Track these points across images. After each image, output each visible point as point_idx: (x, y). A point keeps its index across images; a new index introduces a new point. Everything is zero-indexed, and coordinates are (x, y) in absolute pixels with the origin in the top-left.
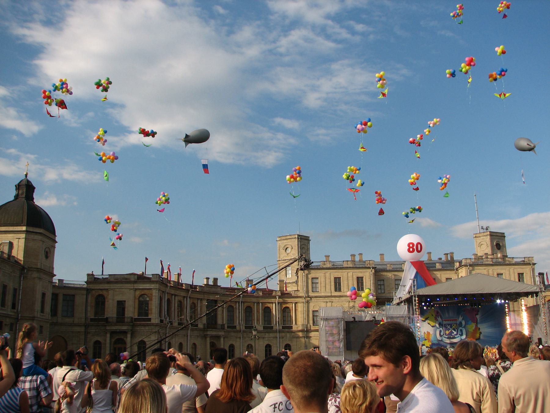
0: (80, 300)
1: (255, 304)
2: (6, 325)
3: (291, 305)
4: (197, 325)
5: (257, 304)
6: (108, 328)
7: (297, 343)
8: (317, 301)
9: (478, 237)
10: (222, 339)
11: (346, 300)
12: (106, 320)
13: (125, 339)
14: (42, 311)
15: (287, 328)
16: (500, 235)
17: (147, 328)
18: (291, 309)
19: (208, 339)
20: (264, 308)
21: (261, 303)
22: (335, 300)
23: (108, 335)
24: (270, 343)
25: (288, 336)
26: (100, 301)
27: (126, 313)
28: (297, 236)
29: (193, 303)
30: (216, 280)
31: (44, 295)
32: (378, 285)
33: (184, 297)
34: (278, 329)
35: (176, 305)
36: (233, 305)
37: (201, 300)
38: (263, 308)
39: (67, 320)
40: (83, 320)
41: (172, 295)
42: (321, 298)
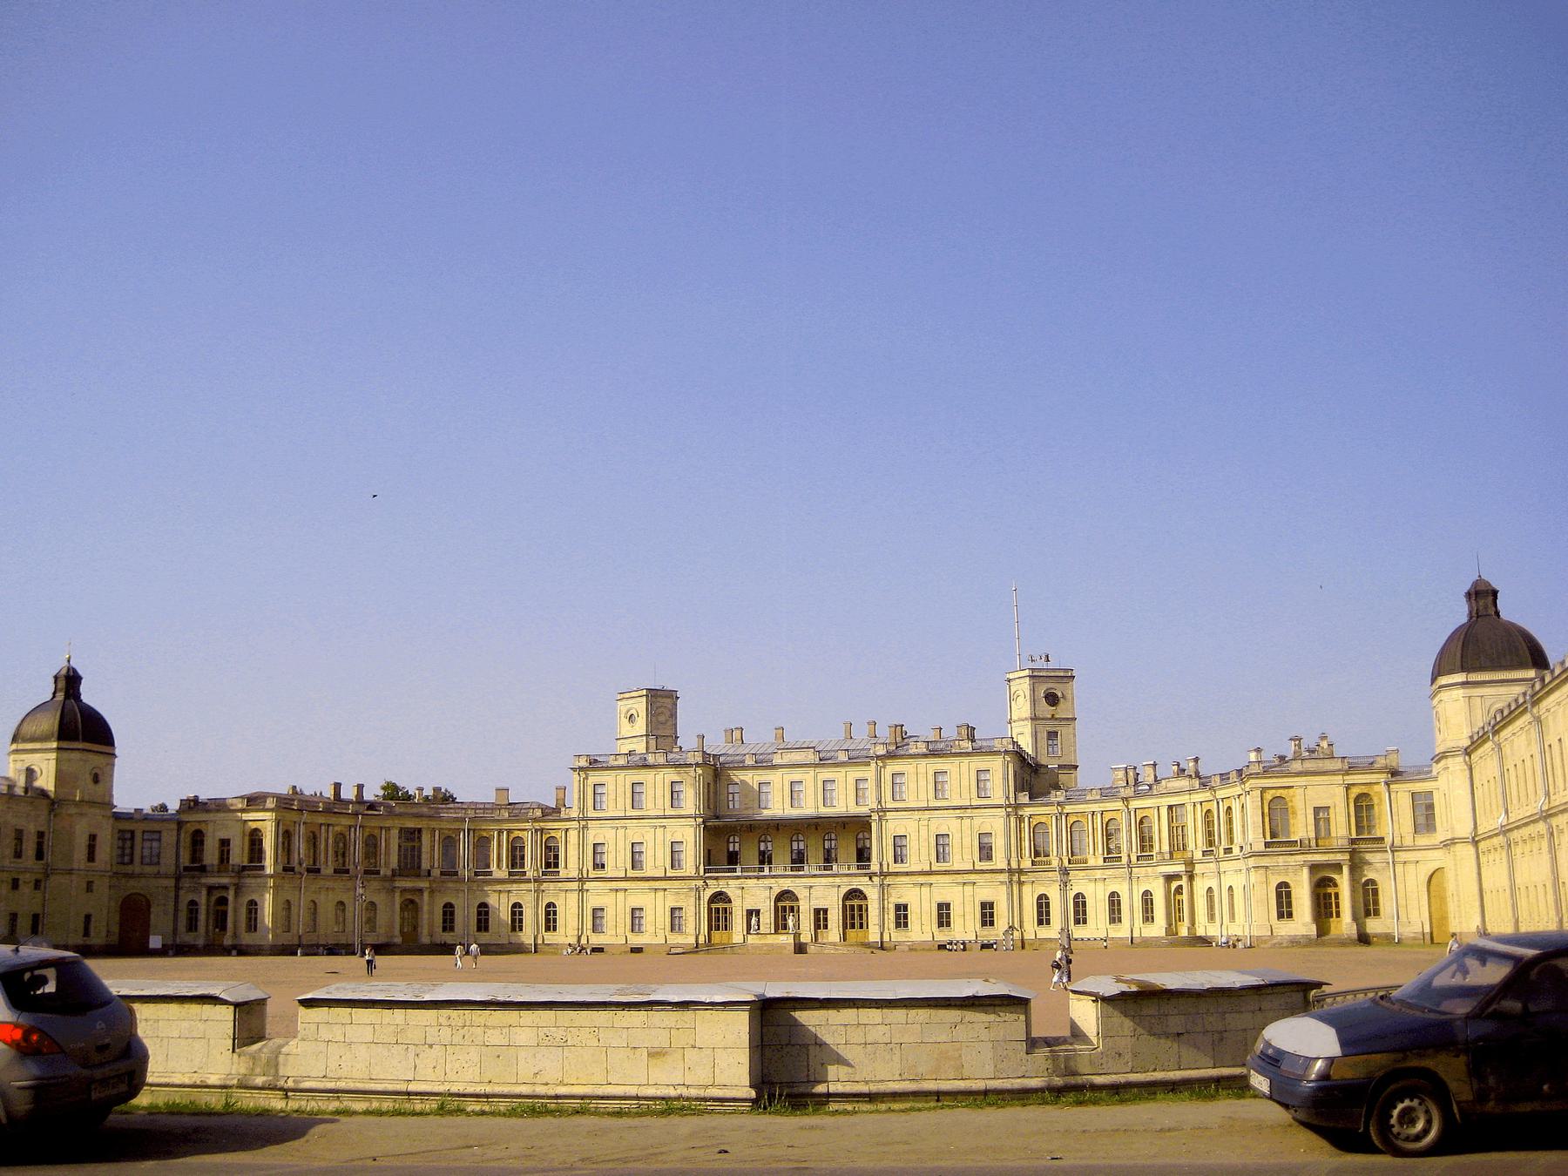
0: (169, 837)
2: (25, 882)
4: (378, 873)
6: (203, 881)
10: (426, 895)
12: (203, 869)
14: (91, 857)
19: (397, 894)
23: (204, 892)
26: (198, 838)
28: (644, 692)
29: (372, 836)
31: (93, 838)
33: (350, 827)
37: (388, 829)
39: (149, 869)
40: (173, 868)
41: (321, 824)
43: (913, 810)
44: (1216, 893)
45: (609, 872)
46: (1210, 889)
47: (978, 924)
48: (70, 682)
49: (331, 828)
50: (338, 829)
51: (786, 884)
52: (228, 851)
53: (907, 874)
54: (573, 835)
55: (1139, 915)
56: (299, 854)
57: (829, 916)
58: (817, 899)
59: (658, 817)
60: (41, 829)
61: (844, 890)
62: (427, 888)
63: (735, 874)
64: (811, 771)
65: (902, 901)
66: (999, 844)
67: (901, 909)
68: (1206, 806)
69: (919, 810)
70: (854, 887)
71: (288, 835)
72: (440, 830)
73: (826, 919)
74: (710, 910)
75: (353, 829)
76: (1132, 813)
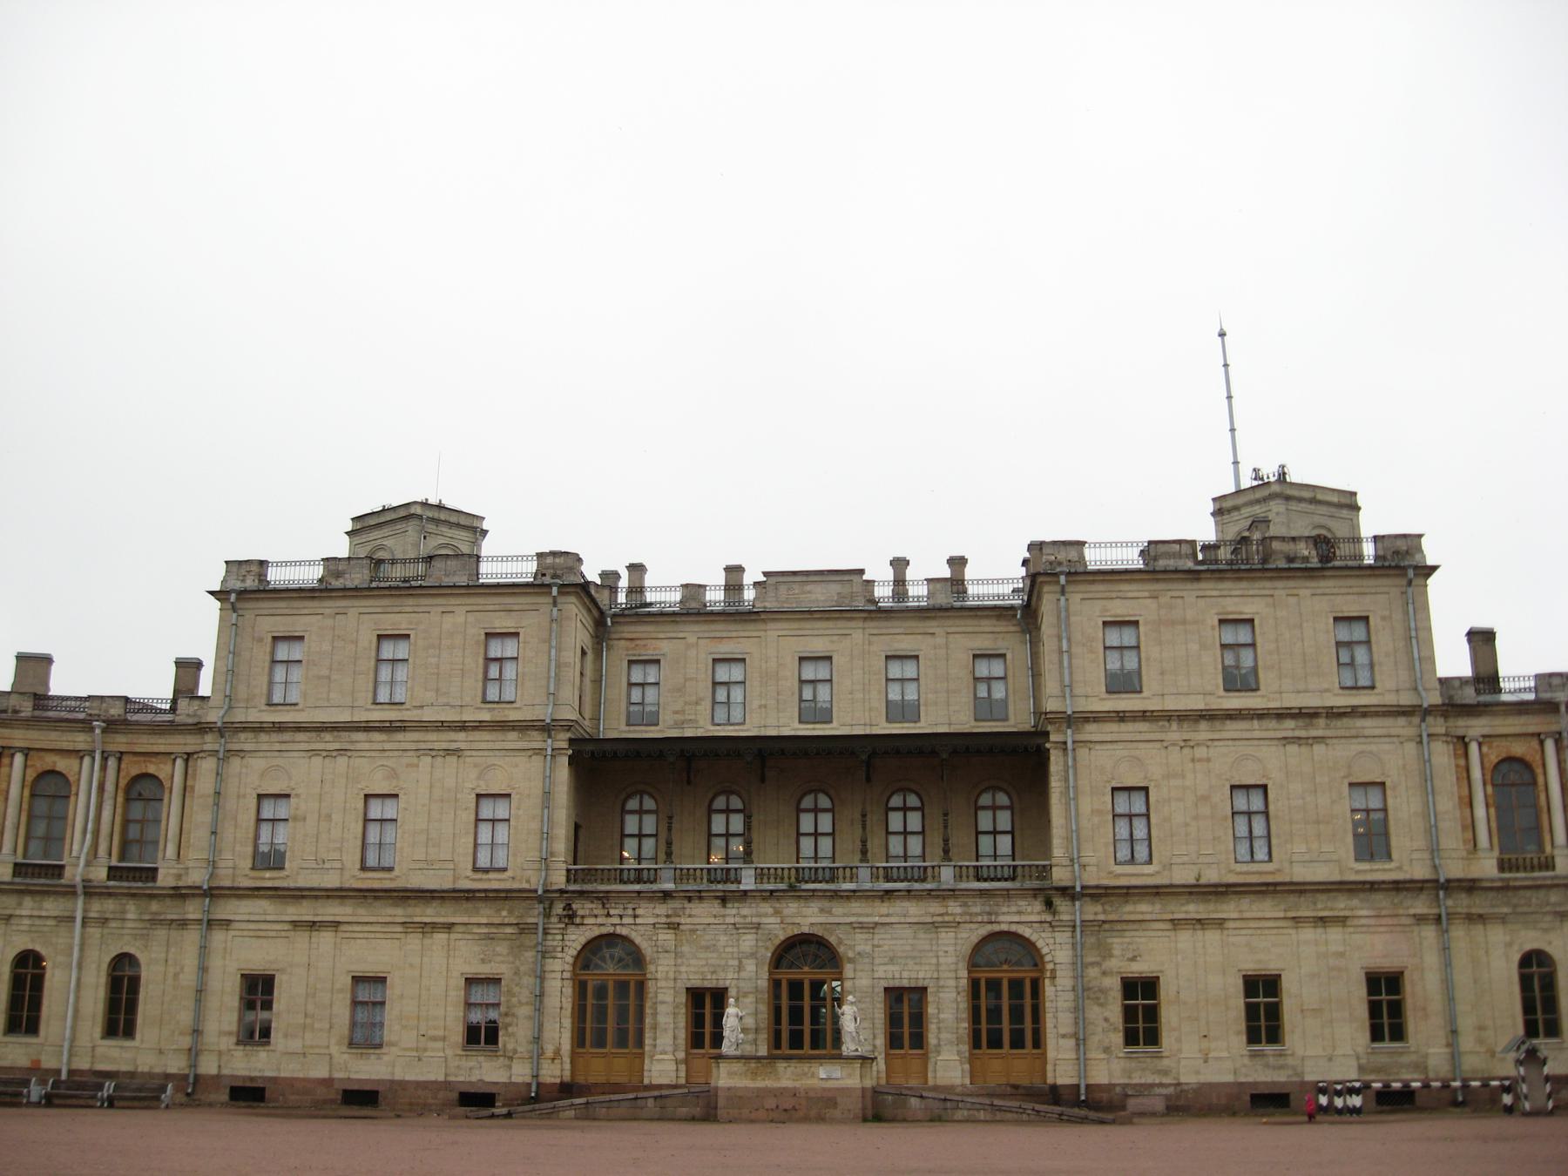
3: (168, 768)
7: (167, 952)
8: (284, 747)
9: (1229, 511)
11: (423, 746)
15: (137, 875)
16: (1335, 499)
18: (167, 784)
20: (35, 775)
21: (27, 752)
22: (366, 746)
24: (38, 948)
25: (130, 916)
32: (631, 685)
34: (78, 879)
38: (31, 775)
42: (301, 736)
43: (1168, 716)
45: (296, 874)
47: (1367, 1035)
51: (807, 917)
53: (1156, 892)
54: (207, 766)
57: (931, 1010)
58: (892, 961)
59: (442, 726)
61: (972, 934)
63: (655, 887)
64: (858, 634)
65: (1140, 968)
66: (1404, 808)
69: (1184, 717)
70: (1004, 927)
73: (919, 1019)
74: (581, 988)
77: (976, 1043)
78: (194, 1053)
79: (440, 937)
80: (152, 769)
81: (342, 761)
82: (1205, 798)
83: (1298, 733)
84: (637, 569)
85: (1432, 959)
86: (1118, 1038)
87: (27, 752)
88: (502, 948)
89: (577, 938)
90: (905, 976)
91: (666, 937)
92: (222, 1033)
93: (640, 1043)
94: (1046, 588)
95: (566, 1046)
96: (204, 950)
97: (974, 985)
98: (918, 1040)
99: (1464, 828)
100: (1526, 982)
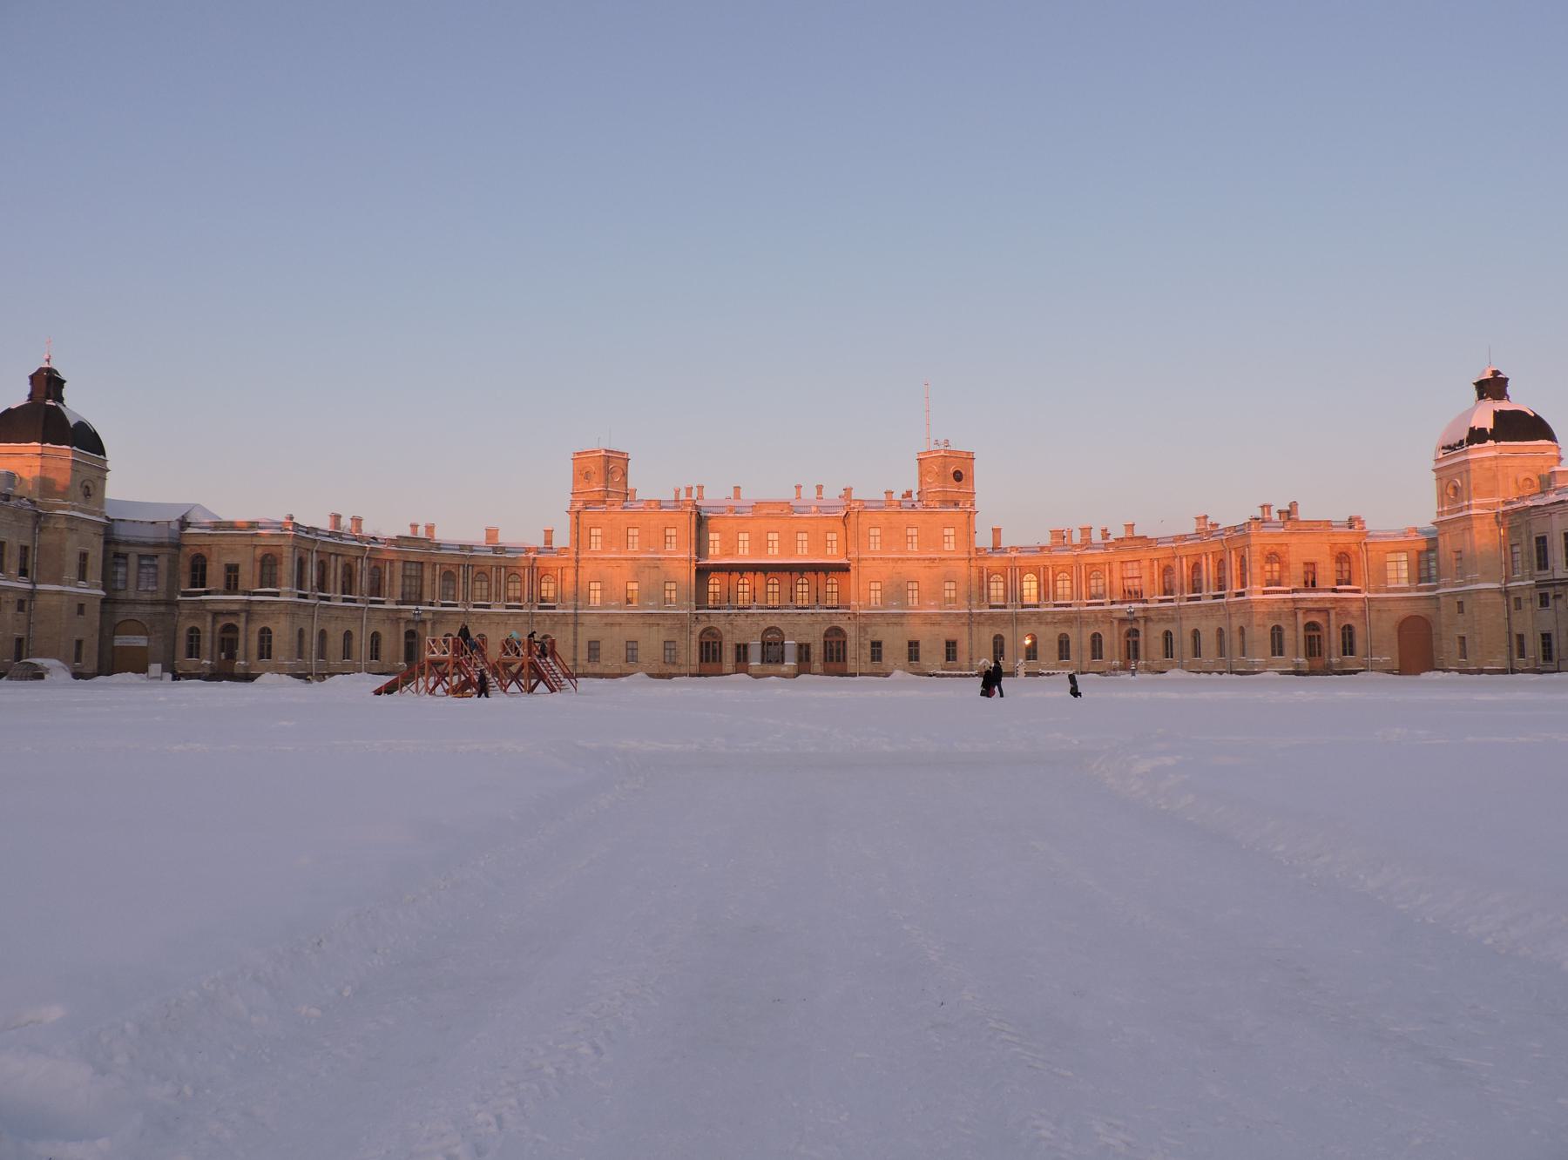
1: (494, 569)
2: (7, 602)
5: (497, 569)
10: (429, 625)
13: (237, 624)
17: (273, 607)
19: (402, 625)
21: (505, 567)
23: (209, 619)
27: (240, 583)
30: (430, 528)
31: (84, 556)
33: (357, 557)
35: (339, 571)
36: (453, 570)
41: (331, 554)
44: (1226, 635)
46: (1168, 635)
47: (945, 659)
48: (48, 383)
49: (340, 558)
50: (347, 559)
52: (236, 578)
55: (1088, 654)
56: (312, 581)
57: (812, 650)
58: (800, 635)
60: (26, 543)
62: (430, 620)
65: (876, 639)
67: (876, 645)
68: (1166, 562)
71: (301, 563)
72: (441, 564)
73: (808, 653)
75: (359, 560)
76: (1083, 567)
77: (825, 660)
78: (575, 666)
79: (655, 628)
80: (550, 572)
81: (619, 569)
82: (899, 586)
83: (931, 565)
84: (701, 488)
85: (966, 637)
86: (869, 659)
87: (505, 567)
88: (676, 631)
89: (699, 628)
90: (804, 640)
91: (728, 627)
92: (583, 660)
93: (720, 661)
94: (851, 516)
95: (698, 662)
96: (575, 634)
97: (825, 642)
98: (808, 659)
99: (980, 596)
100: (995, 644)
